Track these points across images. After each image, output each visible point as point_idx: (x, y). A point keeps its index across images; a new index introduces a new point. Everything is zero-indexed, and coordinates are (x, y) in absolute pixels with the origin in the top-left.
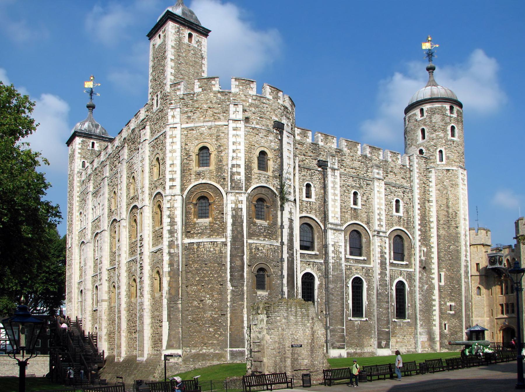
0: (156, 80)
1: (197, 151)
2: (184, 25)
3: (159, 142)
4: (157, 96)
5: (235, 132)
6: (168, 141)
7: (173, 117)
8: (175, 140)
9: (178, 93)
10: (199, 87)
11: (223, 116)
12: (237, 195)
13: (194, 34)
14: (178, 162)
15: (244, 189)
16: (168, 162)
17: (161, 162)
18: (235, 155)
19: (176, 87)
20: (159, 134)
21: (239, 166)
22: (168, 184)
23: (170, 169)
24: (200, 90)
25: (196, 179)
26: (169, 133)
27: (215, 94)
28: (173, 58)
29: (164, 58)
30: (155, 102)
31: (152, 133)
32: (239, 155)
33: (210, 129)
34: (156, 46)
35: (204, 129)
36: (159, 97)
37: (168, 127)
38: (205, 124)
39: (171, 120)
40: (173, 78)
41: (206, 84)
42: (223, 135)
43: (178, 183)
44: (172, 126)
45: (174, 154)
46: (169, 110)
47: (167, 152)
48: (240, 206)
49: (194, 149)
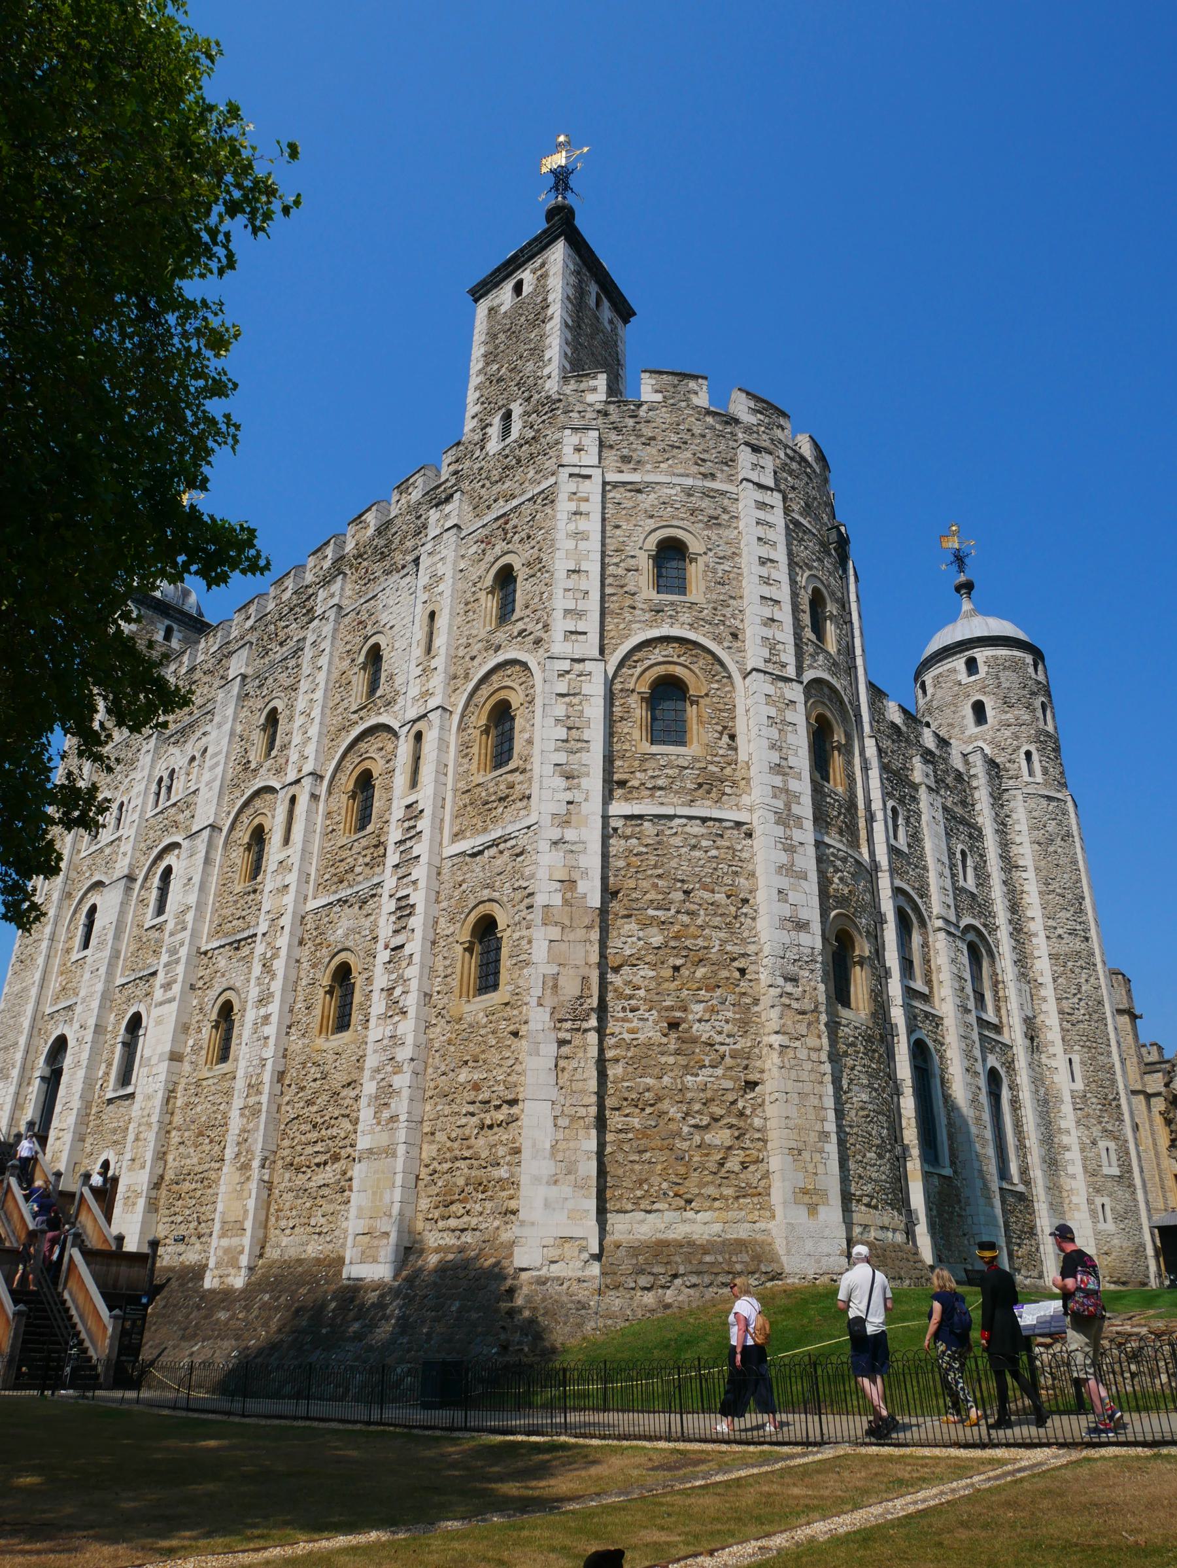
0: (499, 380)
1: (652, 543)
2: (589, 270)
3: (511, 523)
4: (508, 416)
5: (761, 515)
6: (564, 506)
7: (578, 449)
8: (584, 507)
9: (590, 398)
10: (657, 391)
11: (722, 471)
12: (781, 684)
13: (606, 304)
14: (594, 568)
15: (791, 672)
16: (560, 565)
17: (521, 573)
18: (764, 571)
19: (583, 386)
20: (515, 503)
21: (777, 602)
22: (560, 625)
23: (570, 584)
24: (658, 397)
25: (650, 624)
26: (567, 486)
27: (699, 413)
28: (570, 323)
29: (540, 318)
30: (494, 431)
31: (479, 506)
32: (775, 575)
33: (690, 495)
34: (503, 309)
35: (673, 492)
36: (517, 409)
37: (564, 473)
38: (676, 480)
39: (569, 456)
40: (568, 367)
41: (675, 386)
42: (726, 517)
43: (591, 624)
44: (576, 470)
45: (583, 545)
46: (568, 432)
47: (560, 535)
48: (790, 716)
49: (640, 544)
